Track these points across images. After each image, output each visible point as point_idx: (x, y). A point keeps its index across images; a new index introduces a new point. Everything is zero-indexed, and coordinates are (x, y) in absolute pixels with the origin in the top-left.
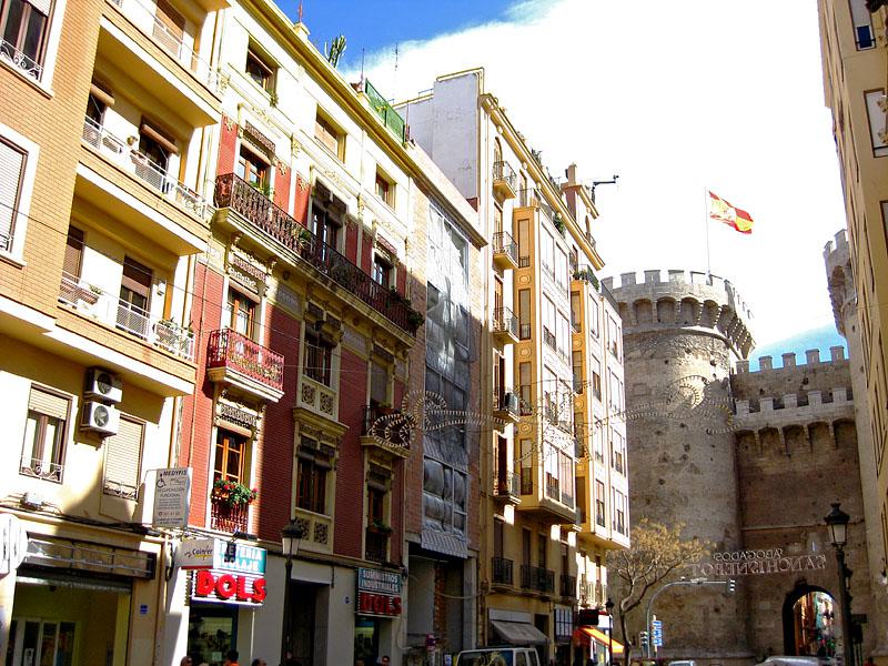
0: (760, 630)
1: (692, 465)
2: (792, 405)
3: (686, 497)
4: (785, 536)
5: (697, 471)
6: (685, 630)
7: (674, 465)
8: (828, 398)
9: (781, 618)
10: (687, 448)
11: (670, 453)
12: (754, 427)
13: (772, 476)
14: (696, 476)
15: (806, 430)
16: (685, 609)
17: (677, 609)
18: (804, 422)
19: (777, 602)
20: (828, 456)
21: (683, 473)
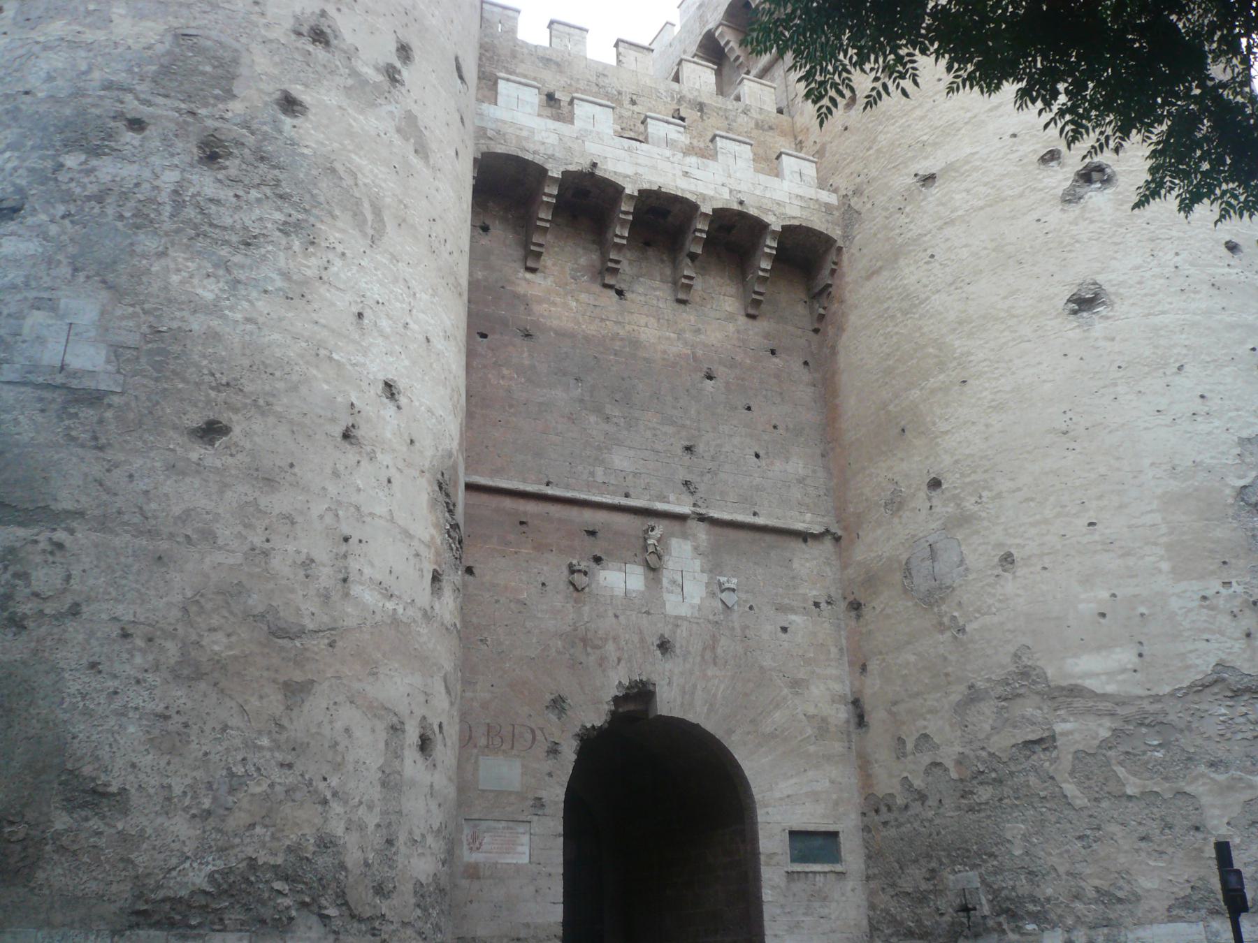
0: (473, 872)
1: (410, 118)
2: (669, 143)
3: (377, 211)
4: (592, 533)
5: (421, 150)
6: (302, 823)
7: (354, 73)
8: (770, 163)
9: (556, 824)
10: (404, 51)
11: (346, 26)
12: (552, 157)
13: (561, 334)
14: (415, 160)
15: (702, 225)
16: (315, 706)
17: (274, 702)
18: (704, 197)
19: (548, 765)
20: (731, 328)
21: (376, 122)
